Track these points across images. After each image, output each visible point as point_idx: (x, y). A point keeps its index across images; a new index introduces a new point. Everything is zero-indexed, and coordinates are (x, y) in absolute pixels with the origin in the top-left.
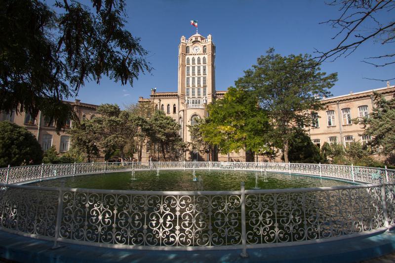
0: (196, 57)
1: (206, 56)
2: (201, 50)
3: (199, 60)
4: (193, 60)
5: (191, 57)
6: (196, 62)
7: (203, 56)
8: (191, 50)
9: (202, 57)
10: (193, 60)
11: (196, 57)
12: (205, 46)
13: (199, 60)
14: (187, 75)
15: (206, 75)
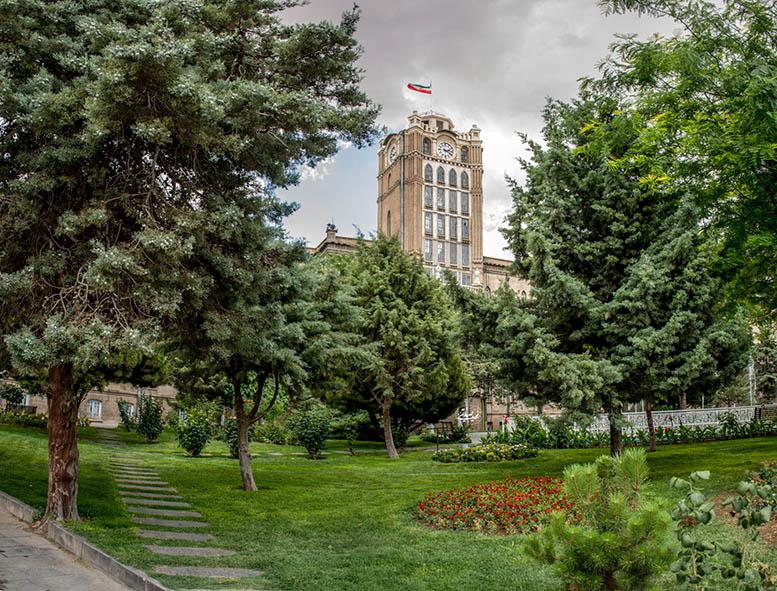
0: (447, 168)
1: (469, 172)
2: (457, 152)
3: (453, 173)
4: (441, 172)
5: (435, 166)
6: (447, 181)
7: (462, 169)
8: (437, 148)
9: (459, 171)
10: (441, 172)
11: (447, 168)
12: (464, 147)
13: (453, 173)
14: (427, 207)
15: (468, 215)
